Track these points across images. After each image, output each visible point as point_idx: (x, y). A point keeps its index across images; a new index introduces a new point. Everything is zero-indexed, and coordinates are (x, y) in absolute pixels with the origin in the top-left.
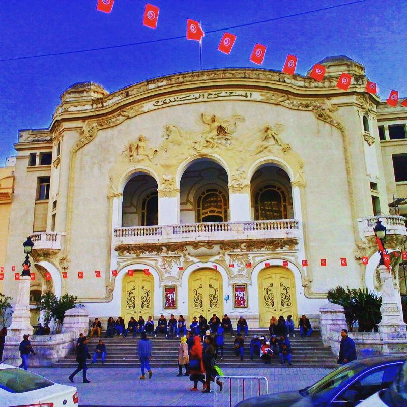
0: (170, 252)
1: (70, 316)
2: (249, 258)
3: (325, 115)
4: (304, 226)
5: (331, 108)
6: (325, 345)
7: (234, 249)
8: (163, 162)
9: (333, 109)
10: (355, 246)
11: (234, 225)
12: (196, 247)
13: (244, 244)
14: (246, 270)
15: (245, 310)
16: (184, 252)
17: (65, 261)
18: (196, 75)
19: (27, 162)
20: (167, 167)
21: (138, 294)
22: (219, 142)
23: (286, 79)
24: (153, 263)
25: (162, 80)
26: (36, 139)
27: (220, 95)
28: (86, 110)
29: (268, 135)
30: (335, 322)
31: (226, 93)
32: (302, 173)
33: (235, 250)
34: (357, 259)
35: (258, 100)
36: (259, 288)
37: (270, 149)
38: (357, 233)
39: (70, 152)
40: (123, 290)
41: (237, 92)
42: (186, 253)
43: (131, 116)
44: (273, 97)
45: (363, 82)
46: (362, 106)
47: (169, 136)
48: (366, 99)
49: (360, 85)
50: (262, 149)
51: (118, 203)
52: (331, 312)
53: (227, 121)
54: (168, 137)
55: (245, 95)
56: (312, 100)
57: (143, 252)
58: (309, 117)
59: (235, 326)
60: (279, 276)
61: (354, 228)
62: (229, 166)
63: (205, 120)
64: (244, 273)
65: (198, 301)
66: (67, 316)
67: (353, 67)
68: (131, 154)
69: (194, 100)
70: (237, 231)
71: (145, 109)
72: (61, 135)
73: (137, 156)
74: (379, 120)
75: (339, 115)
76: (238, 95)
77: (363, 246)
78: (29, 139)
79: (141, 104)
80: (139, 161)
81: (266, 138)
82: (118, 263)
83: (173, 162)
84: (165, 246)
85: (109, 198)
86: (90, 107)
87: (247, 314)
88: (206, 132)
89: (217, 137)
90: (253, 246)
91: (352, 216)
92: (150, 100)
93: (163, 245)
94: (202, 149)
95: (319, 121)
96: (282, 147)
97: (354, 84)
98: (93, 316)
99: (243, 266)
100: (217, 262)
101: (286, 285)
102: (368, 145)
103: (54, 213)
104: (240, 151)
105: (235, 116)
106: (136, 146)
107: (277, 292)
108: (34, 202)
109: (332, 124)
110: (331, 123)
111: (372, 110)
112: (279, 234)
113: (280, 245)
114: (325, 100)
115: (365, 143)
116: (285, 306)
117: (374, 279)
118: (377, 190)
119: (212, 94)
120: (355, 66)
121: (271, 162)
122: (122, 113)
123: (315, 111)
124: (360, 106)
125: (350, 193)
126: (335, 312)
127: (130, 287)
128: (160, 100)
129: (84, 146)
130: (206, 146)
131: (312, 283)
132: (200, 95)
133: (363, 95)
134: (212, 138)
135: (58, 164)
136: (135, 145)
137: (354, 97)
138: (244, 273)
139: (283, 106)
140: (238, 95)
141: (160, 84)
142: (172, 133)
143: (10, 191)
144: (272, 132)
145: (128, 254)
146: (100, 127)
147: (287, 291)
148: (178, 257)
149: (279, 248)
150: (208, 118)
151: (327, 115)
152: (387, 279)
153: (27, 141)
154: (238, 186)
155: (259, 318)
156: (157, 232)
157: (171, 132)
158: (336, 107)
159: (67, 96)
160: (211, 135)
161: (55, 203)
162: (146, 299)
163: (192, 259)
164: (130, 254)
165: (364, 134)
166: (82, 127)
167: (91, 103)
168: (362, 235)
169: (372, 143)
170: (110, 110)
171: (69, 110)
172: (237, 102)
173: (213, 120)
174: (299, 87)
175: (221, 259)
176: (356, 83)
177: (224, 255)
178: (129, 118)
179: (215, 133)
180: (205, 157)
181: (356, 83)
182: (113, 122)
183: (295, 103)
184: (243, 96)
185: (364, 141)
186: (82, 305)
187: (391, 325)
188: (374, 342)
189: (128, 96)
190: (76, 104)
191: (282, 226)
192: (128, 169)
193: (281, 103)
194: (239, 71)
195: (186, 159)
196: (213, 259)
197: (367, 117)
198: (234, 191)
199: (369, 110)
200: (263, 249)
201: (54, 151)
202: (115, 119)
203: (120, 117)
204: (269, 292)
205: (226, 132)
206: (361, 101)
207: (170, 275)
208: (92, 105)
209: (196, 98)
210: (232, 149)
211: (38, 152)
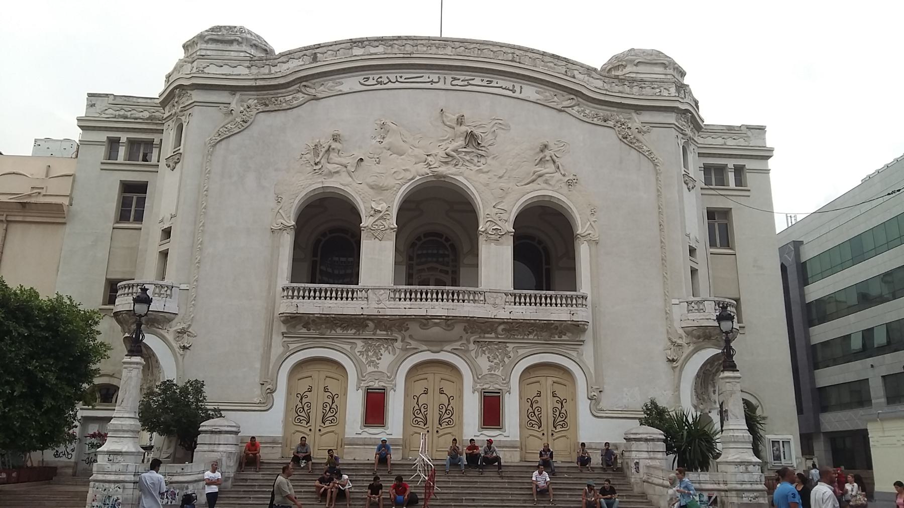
0: (378, 332)
1: (212, 432)
3: (632, 137)
4: (594, 307)
5: (639, 125)
6: (637, 490)
8: (371, 180)
9: (643, 128)
10: (667, 339)
11: (488, 293)
12: (425, 325)
13: (502, 327)
14: (502, 368)
15: (498, 432)
16: (403, 332)
17: (185, 336)
18: (435, 44)
19: (102, 151)
20: (378, 189)
21: (317, 400)
22: (468, 158)
23: (576, 73)
24: (348, 347)
25: (376, 43)
26: (122, 112)
27: (471, 82)
28: (240, 75)
29: (545, 157)
30: (652, 455)
31: (482, 80)
32: (595, 221)
34: (669, 360)
35: (531, 99)
36: (521, 398)
37: (547, 180)
38: (670, 320)
39: (205, 144)
40: (289, 392)
42: (407, 334)
43: (319, 95)
44: (555, 97)
45: (685, 94)
46: (682, 130)
47: (384, 138)
48: (687, 120)
49: (682, 98)
50: (534, 177)
51: (287, 241)
52: (646, 440)
53: (481, 126)
54: (382, 140)
55: (511, 88)
56: (614, 111)
57: (332, 329)
58: (608, 138)
59: (596, 459)
60: (550, 381)
61: (667, 313)
63: (445, 119)
65: (420, 416)
66: (206, 432)
67: (672, 69)
68: (317, 160)
69: (429, 85)
70: (495, 305)
71: (345, 88)
72: (182, 113)
73: (328, 164)
74: (700, 155)
75: (651, 140)
76: (501, 87)
77: (679, 341)
78: (106, 112)
79: (335, 79)
80: (331, 174)
81: (541, 159)
82: (286, 345)
83: (390, 182)
84: (372, 320)
85: (273, 231)
86: (247, 71)
87: (502, 438)
88: (445, 140)
89: (464, 150)
90: (517, 330)
91: (665, 294)
92: (354, 74)
93: (369, 318)
94: (439, 166)
95: (622, 143)
97: (675, 96)
98: (248, 431)
99: (495, 361)
100: (453, 351)
101: (561, 394)
102: (688, 191)
103: (163, 248)
104: (500, 177)
105: (494, 119)
106: (326, 148)
107: (547, 405)
108: (111, 225)
109: (641, 153)
110: (639, 151)
111: (693, 139)
112: (559, 314)
113: (558, 331)
114: (633, 114)
115: (685, 186)
116: (559, 428)
117: (692, 391)
118: (696, 258)
119: (459, 79)
120: (674, 69)
121: (547, 199)
122: (303, 89)
123: (617, 128)
124: (680, 131)
125: (662, 259)
126: (653, 440)
127: (302, 387)
128: (371, 77)
129: (229, 137)
130: (446, 163)
131: (602, 393)
132: (439, 78)
133: (684, 114)
134: (456, 151)
135: (176, 163)
136: (324, 145)
137: (674, 115)
139: (567, 112)
140: (501, 87)
141: (373, 50)
142: (389, 135)
143: (65, 201)
144: (550, 151)
145: (304, 330)
146: (261, 108)
147: (562, 404)
148: (393, 339)
149: (556, 336)
150: (452, 117)
152: (735, 393)
153: (103, 115)
155: (518, 444)
156: (355, 295)
157: (388, 131)
158: (648, 126)
159: (204, 46)
160: (455, 145)
161: (167, 233)
162: (330, 408)
163: (414, 344)
164: (309, 330)
165: (684, 173)
166: (230, 104)
167: (247, 64)
168: (677, 325)
169: (693, 188)
170: (282, 81)
171: (206, 70)
172: (499, 96)
173: (460, 121)
174: (596, 88)
175: (463, 348)
176: (677, 95)
178: (316, 98)
179: (460, 142)
180: (442, 179)
181: (677, 95)
182: (286, 102)
183: (587, 111)
185: (683, 183)
186: (218, 413)
187: (741, 462)
188: (716, 487)
189: (317, 62)
190: (220, 62)
191: (564, 301)
192: (310, 185)
193: (566, 109)
194: (504, 49)
195: (412, 179)
196: (448, 348)
197: (686, 147)
198: (488, 240)
199: (690, 138)
200: (531, 337)
201: (169, 137)
202: (291, 97)
203: (300, 95)
204: (535, 406)
205: (479, 144)
206: (682, 123)
207: (376, 370)
208: (248, 67)
209: (432, 82)
210: (488, 172)
211: (124, 137)
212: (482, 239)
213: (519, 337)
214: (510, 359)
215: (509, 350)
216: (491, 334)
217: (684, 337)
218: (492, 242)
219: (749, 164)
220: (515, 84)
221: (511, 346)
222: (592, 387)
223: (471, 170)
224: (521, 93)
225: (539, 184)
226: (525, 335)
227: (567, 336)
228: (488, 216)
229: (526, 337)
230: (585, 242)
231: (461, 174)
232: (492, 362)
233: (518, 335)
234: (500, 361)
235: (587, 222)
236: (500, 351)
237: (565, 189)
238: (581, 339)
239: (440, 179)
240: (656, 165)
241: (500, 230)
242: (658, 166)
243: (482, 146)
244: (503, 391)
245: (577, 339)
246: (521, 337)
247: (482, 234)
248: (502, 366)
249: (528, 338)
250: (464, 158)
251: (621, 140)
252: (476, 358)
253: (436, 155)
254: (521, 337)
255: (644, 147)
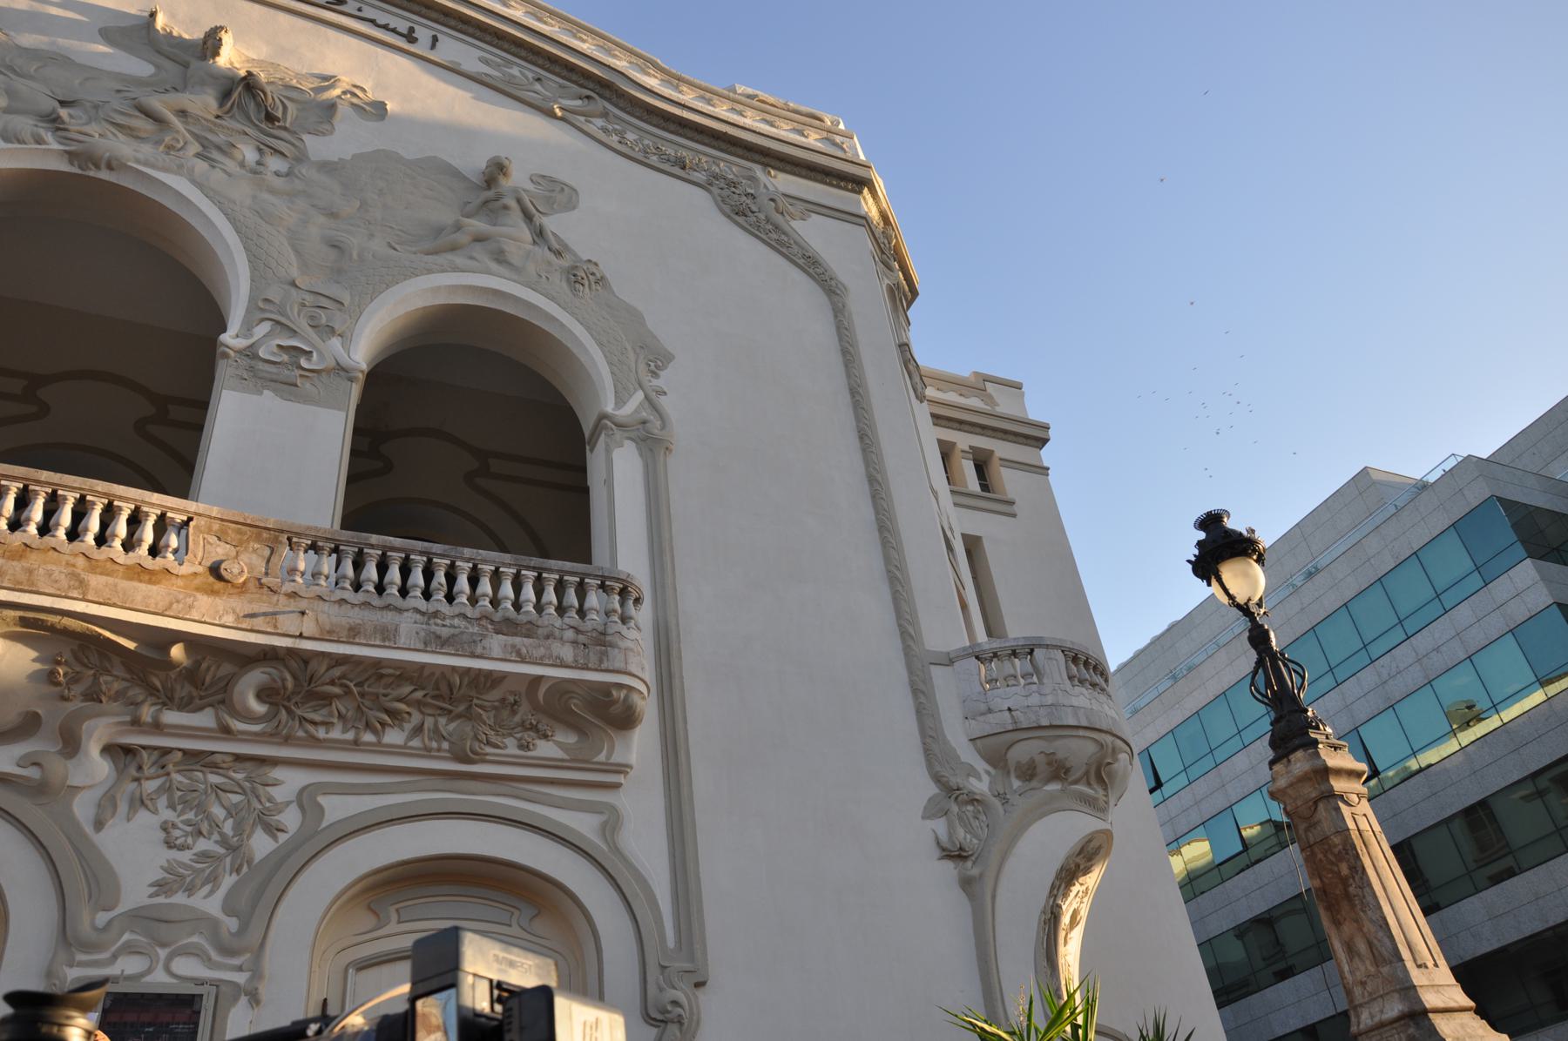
2: (279, 793)
3: (762, 216)
7: (168, 700)
13: (256, 677)
14: (228, 881)
33: (171, 717)
41: (365, 8)
44: (538, 86)
46: (883, 253)
55: (405, 32)
62: (253, 259)
64: (210, 903)
76: (373, 21)
81: (486, 202)
96: (565, 263)
99: (203, 845)
113: (517, 719)
138: (210, 903)
140: (373, 21)
151: (768, 220)
154: (285, 358)
168: (957, 735)
175: (33, 773)
177: (71, 744)
180: (104, 175)
183: (631, 136)
184: (394, 31)
200: (393, 737)
205: (270, 118)
212: (224, 371)
213: (336, 734)
214: (283, 837)
215: (279, 799)
216: (201, 709)
217: (986, 779)
218: (274, 391)
219: (1002, 449)
220: (416, 27)
221: (290, 782)
222: (664, 968)
223: (225, 171)
224: (433, 46)
225: (472, 258)
226: (368, 726)
227: (560, 745)
228: (267, 307)
229: (368, 737)
230: (628, 443)
231: (179, 170)
232: (182, 848)
233: (328, 725)
234: (224, 842)
235: (636, 390)
236: (235, 798)
237: (560, 285)
238: (617, 758)
239: (92, 173)
240: (834, 292)
241: (311, 352)
242: (838, 294)
243: (280, 127)
244: (223, 988)
245: (602, 757)
246: (350, 736)
247: (225, 356)
248: (238, 871)
249: (379, 743)
250: (207, 139)
251: (728, 217)
252: (99, 825)
253: (96, 107)
254: (350, 736)
255: (794, 246)
